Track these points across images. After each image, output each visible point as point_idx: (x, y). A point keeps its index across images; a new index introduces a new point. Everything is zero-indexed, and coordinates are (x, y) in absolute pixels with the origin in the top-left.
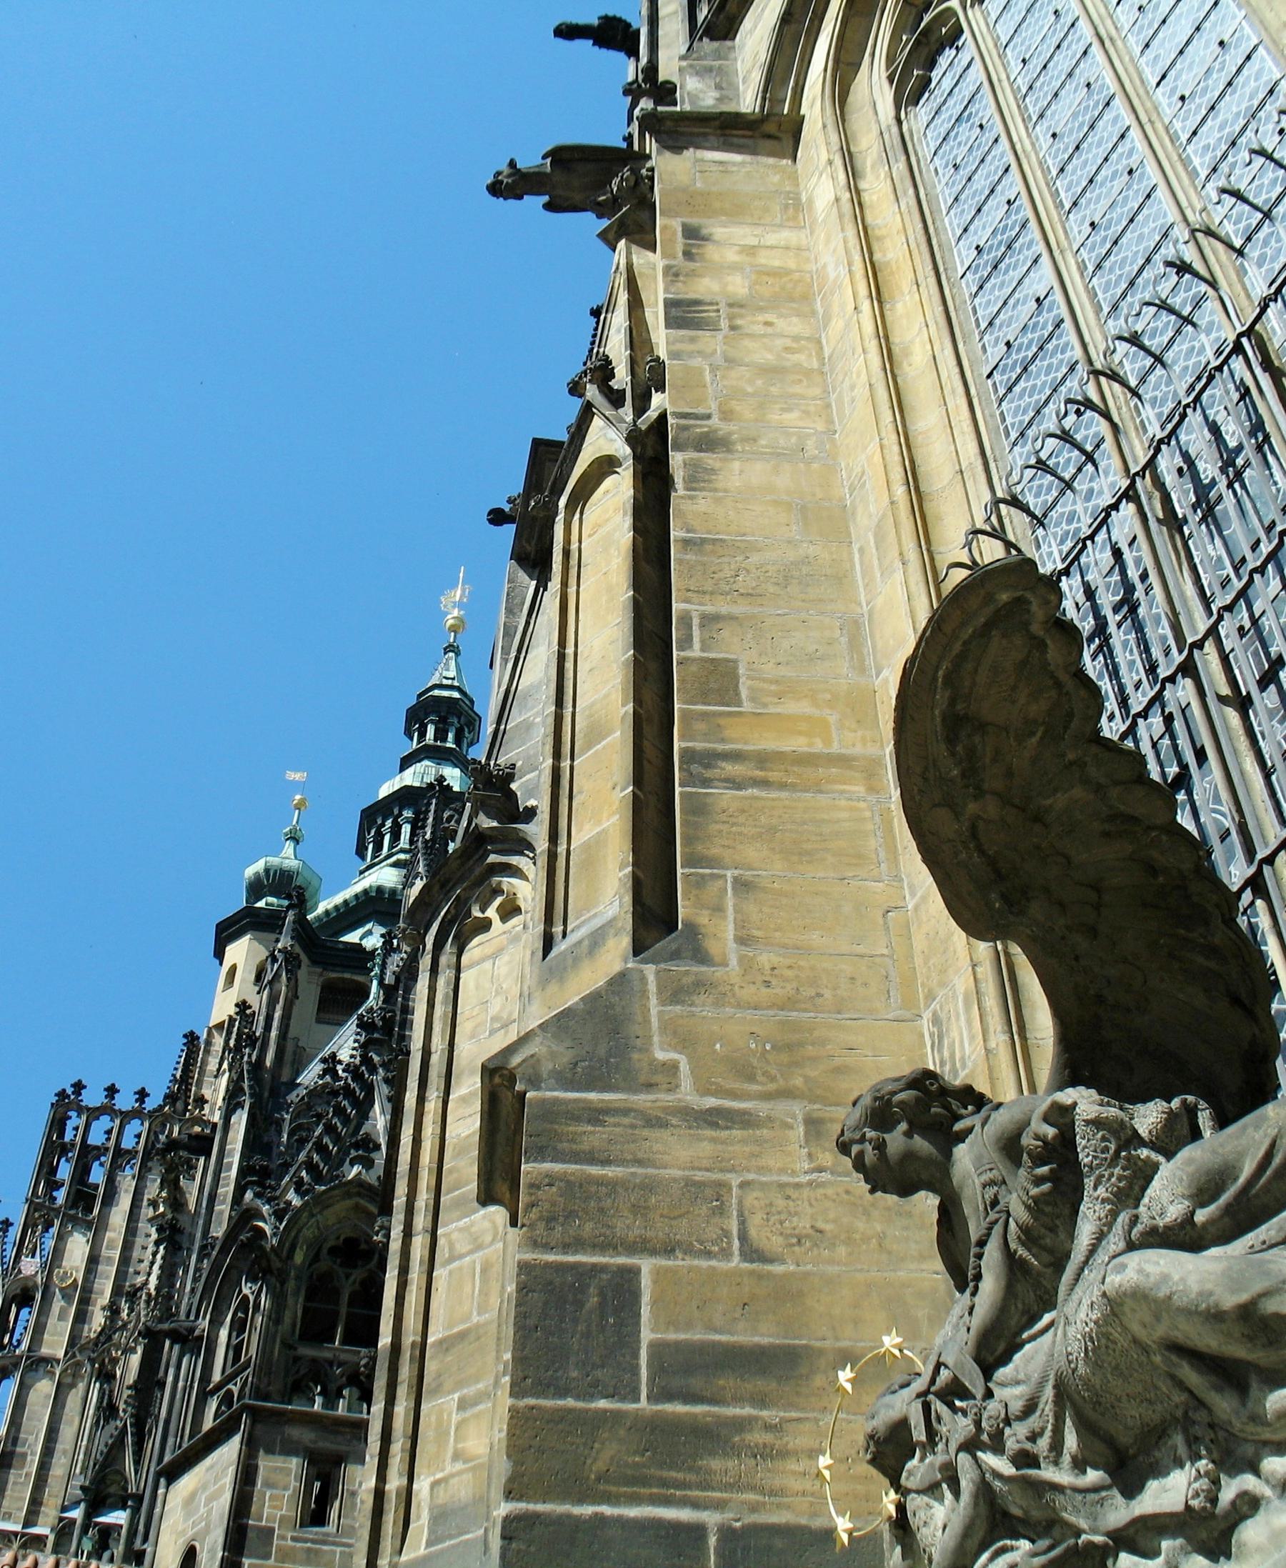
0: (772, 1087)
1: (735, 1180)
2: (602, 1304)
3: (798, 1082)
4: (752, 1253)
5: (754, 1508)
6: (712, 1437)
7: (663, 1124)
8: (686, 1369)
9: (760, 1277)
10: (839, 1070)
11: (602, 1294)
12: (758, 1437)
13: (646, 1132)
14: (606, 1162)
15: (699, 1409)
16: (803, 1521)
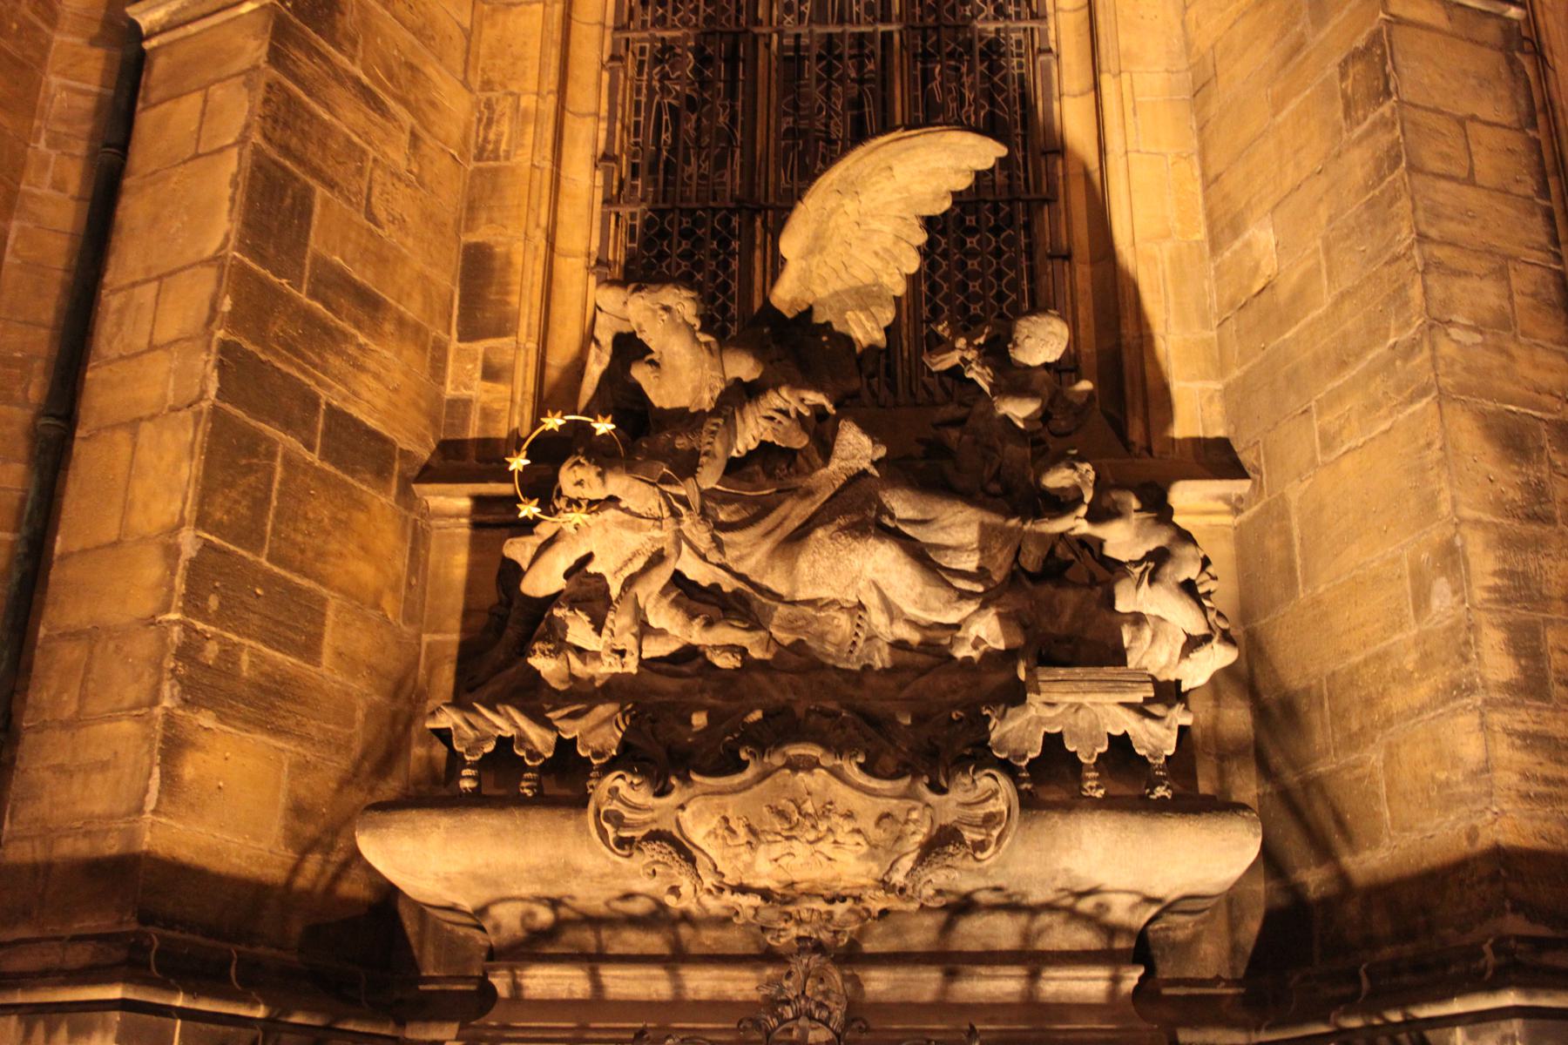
0: (398, 92)
1: (372, 153)
3: (412, 98)
4: (371, 217)
5: (345, 399)
6: (330, 337)
7: (342, 84)
8: (333, 283)
10: (433, 104)
11: (294, 198)
12: (351, 350)
13: (334, 83)
14: (310, 94)
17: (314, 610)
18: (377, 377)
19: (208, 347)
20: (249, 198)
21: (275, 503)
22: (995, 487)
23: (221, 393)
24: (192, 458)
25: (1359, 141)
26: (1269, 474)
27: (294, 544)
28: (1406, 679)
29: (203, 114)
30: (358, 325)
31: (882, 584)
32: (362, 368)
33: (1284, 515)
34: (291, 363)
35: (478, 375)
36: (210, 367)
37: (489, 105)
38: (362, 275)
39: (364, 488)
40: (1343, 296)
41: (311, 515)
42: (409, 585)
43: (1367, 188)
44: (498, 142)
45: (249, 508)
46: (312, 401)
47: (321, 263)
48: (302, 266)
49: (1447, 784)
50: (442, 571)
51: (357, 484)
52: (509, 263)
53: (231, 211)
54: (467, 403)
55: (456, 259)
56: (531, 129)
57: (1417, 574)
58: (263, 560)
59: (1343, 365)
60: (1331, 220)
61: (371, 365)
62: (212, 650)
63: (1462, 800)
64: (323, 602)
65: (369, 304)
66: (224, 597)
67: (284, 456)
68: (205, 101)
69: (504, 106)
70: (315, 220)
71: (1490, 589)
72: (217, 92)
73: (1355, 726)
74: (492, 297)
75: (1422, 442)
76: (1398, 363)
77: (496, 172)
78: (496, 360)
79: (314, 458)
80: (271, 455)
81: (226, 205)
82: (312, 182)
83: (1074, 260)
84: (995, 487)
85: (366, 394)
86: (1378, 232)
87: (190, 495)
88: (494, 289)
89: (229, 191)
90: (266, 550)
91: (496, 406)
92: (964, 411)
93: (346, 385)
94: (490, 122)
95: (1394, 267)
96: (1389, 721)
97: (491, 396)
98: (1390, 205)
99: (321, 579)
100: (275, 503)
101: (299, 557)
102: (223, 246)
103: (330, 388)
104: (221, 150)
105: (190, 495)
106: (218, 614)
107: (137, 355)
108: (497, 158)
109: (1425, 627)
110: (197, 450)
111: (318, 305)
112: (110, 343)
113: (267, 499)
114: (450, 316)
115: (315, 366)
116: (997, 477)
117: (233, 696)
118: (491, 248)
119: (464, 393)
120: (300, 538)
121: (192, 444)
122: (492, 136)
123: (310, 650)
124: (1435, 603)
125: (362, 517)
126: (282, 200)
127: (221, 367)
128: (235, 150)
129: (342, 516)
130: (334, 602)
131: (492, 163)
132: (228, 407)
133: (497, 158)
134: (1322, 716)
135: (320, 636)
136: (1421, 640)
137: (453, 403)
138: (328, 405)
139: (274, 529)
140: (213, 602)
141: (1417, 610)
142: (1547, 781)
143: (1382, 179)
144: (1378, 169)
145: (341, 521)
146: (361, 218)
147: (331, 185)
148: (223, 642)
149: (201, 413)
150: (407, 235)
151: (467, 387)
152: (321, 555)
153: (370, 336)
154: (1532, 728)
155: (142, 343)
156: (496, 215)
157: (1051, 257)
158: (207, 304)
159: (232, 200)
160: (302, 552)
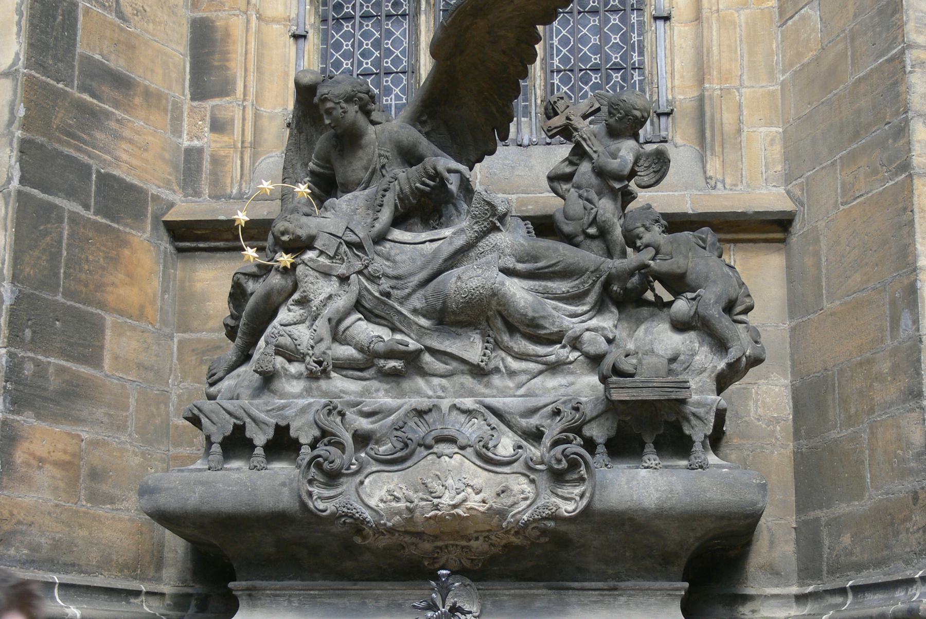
2: (63, 20)
9: (122, 29)
12: (113, 125)
15: (95, 101)
16: (124, 176)
17: (96, 328)
18: (131, 141)
19: (11, 144)
20: (32, 24)
21: (65, 253)
23: (22, 181)
24: (6, 231)
26: (809, 209)
27: (80, 281)
30: (117, 105)
31: (504, 313)
32: (122, 138)
33: (817, 241)
34: (69, 144)
36: (13, 160)
38: (117, 63)
39: (128, 230)
40: (860, 80)
41: (91, 258)
42: (163, 299)
45: (47, 261)
46: (85, 170)
47: (87, 61)
48: (73, 67)
50: (187, 284)
51: (121, 228)
52: (227, 35)
53: (18, 34)
54: (200, 151)
55: (185, 31)
57: (893, 303)
59: (856, 136)
60: (855, 16)
61: (127, 133)
62: (29, 369)
63: (911, 472)
65: (122, 82)
66: (34, 332)
67: (69, 218)
70: (80, 25)
74: (216, 64)
75: (901, 205)
76: (890, 141)
78: (222, 115)
79: (90, 215)
80: (60, 220)
81: (15, 29)
83: (672, 20)
84: (592, 231)
85: (125, 157)
86: (884, 35)
87: (7, 258)
88: (217, 56)
89: (16, 18)
90: (61, 289)
91: (222, 153)
92: (574, 168)
93: (108, 152)
96: (871, 411)
97: (219, 145)
98: (892, 15)
100: (65, 253)
101: (84, 290)
102: (14, 63)
103: (98, 158)
105: (7, 258)
106: (32, 341)
109: (896, 343)
113: (60, 253)
114: (184, 80)
115: (85, 143)
116: (594, 222)
117: (45, 399)
118: (213, 22)
119: (196, 143)
120: (83, 276)
121: (5, 218)
123: (95, 360)
125: (127, 252)
126: (55, 18)
127: (20, 160)
129: (114, 253)
130: (109, 319)
132: (28, 189)
134: (834, 399)
135: (102, 347)
137: (189, 151)
138: (98, 172)
139: (65, 272)
140: (28, 333)
141: (892, 329)
145: (111, 258)
146: (112, 17)
148: (38, 364)
149: (9, 193)
150: (148, 22)
151: (198, 138)
152: (100, 287)
153: (126, 111)
157: (656, 18)
158: (6, 111)
159: (19, 23)
160: (86, 286)
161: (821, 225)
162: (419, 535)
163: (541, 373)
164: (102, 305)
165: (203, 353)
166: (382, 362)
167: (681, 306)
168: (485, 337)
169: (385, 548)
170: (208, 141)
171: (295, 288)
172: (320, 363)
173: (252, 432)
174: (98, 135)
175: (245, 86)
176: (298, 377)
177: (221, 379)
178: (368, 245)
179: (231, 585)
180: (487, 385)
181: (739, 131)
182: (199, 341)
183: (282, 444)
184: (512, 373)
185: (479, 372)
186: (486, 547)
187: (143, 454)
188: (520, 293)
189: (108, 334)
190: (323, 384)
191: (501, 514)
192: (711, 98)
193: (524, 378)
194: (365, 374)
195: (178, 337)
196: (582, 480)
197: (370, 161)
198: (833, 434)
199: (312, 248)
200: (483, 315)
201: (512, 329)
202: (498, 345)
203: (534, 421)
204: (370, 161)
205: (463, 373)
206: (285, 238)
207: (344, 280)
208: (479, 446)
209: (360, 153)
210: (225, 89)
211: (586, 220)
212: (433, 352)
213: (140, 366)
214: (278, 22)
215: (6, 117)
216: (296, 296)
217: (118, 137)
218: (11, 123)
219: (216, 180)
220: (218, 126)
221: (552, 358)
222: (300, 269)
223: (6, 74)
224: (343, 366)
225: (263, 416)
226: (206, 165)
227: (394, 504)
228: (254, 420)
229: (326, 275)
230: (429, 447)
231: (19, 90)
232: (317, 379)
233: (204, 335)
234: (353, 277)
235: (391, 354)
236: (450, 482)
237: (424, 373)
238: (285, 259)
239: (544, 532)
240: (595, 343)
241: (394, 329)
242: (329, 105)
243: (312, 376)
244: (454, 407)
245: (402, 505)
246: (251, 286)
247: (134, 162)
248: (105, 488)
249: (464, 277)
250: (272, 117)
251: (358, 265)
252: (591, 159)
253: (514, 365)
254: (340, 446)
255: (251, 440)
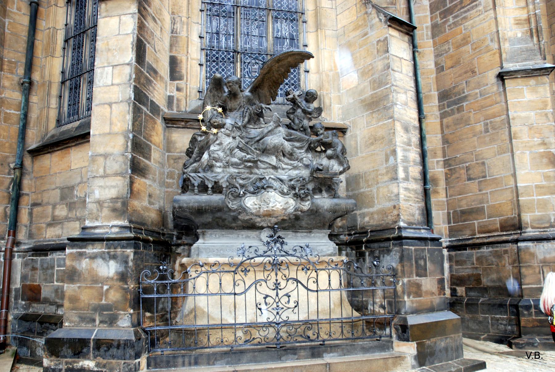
1: (155, 34)
10: (164, 19)
12: (153, 85)
18: (157, 91)
19: (130, 87)
22: (302, 129)
23: (134, 99)
25: (380, 60)
28: (382, 175)
29: (120, 23)
33: (356, 137)
35: (175, 90)
36: (131, 92)
37: (174, 19)
38: (154, 66)
43: (382, 71)
44: (177, 29)
49: (390, 197)
52: (181, 61)
54: (173, 97)
56: (185, 27)
58: (142, 138)
61: (156, 88)
63: (393, 200)
64: (151, 147)
65: (155, 72)
68: (120, 20)
69: (178, 19)
71: (401, 159)
72: (123, 18)
73: (370, 183)
77: (176, 37)
78: (180, 86)
79: (148, 112)
81: (131, 50)
82: (146, 43)
85: (156, 96)
89: (131, 46)
94: (174, 24)
95: (386, 90)
99: (151, 142)
104: (127, 34)
105: (130, 123)
107: (108, 86)
108: (177, 33)
110: (131, 113)
111: (148, 74)
112: (99, 82)
119: (172, 94)
122: (175, 27)
124: (390, 160)
128: (132, 35)
131: (175, 35)
133: (177, 33)
136: (387, 168)
137: (169, 97)
142: (408, 197)
143: (385, 70)
144: (384, 67)
146: (153, 51)
147: (149, 43)
154: (406, 187)
155: (110, 83)
156: (177, 48)
158: (128, 76)
159: (132, 48)
161: (358, 133)
162: (259, 216)
163: (291, 169)
164: (151, 142)
165: (175, 159)
166: (246, 164)
167: (329, 152)
168: (276, 157)
169: (247, 220)
170: (175, 94)
171: (217, 139)
172: (227, 163)
173: (207, 182)
174: (151, 88)
175: (187, 78)
176: (220, 167)
177: (188, 167)
178: (241, 127)
179: (198, 231)
180: (277, 172)
181: (331, 105)
182: (174, 155)
183: (217, 189)
184: (283, 169)
185: (275, 168)
186: (276, 220)
187: (160, 190)
188: (288, 145)
189: (152, 151)
190: (228, 170)
191: (285, 209)
192: (323, 95)
193: (287, 170)
194: (240, 167)
195: (167, 154)
196: (309, 200)
197: (240, 103)
198: (362, 190)
199: (223, 128)
200: (278, 151)
201: (284, 155)
202: (280, 160)
203: (292, 183)
204: (240, 103)
205: (270, 168)
206: (216, 124)
207: (234, 138)
208: (280, 190)
209: (237, 100)
210: (180, 79)
211: (300, 126)
212: (261, 161)
213: (159, 162)
214: (195, 60)
215: (128, 78)
216: (218, 142)
217: (154, 89)
218: (130, 80)
219: (178, 107)
220: (178, 89)
221: (295, 165)
222: (219, 134)
223: (128, 64)
224: (235, 165)
225: (210, 178)
226: (175, 102)
227: (255, 206)
228: (208, 179)
229: (228, 136)
230: (265, 189)
231: (133, 69)
232: (226, 168)
233: (175, 154)
234: (237, 137)
235: (249, 161)
236: (271, 200)
237: (257, 168)
238: (215, 131)
239: (295, 215)
240: (306, 161)
241: (248, 154)
242: (231, 84)
243: (225, 167)
244: (270, 178)
245: (257, 206)
246: (199, 139)
247: (158, 98)
248: (152, 200)
249: (273, 139)
250: (193, 89)
251: (239, 134)
252: (301, 108)
253: (284, 166)
254: (237, 188)
255: (207, 186)
